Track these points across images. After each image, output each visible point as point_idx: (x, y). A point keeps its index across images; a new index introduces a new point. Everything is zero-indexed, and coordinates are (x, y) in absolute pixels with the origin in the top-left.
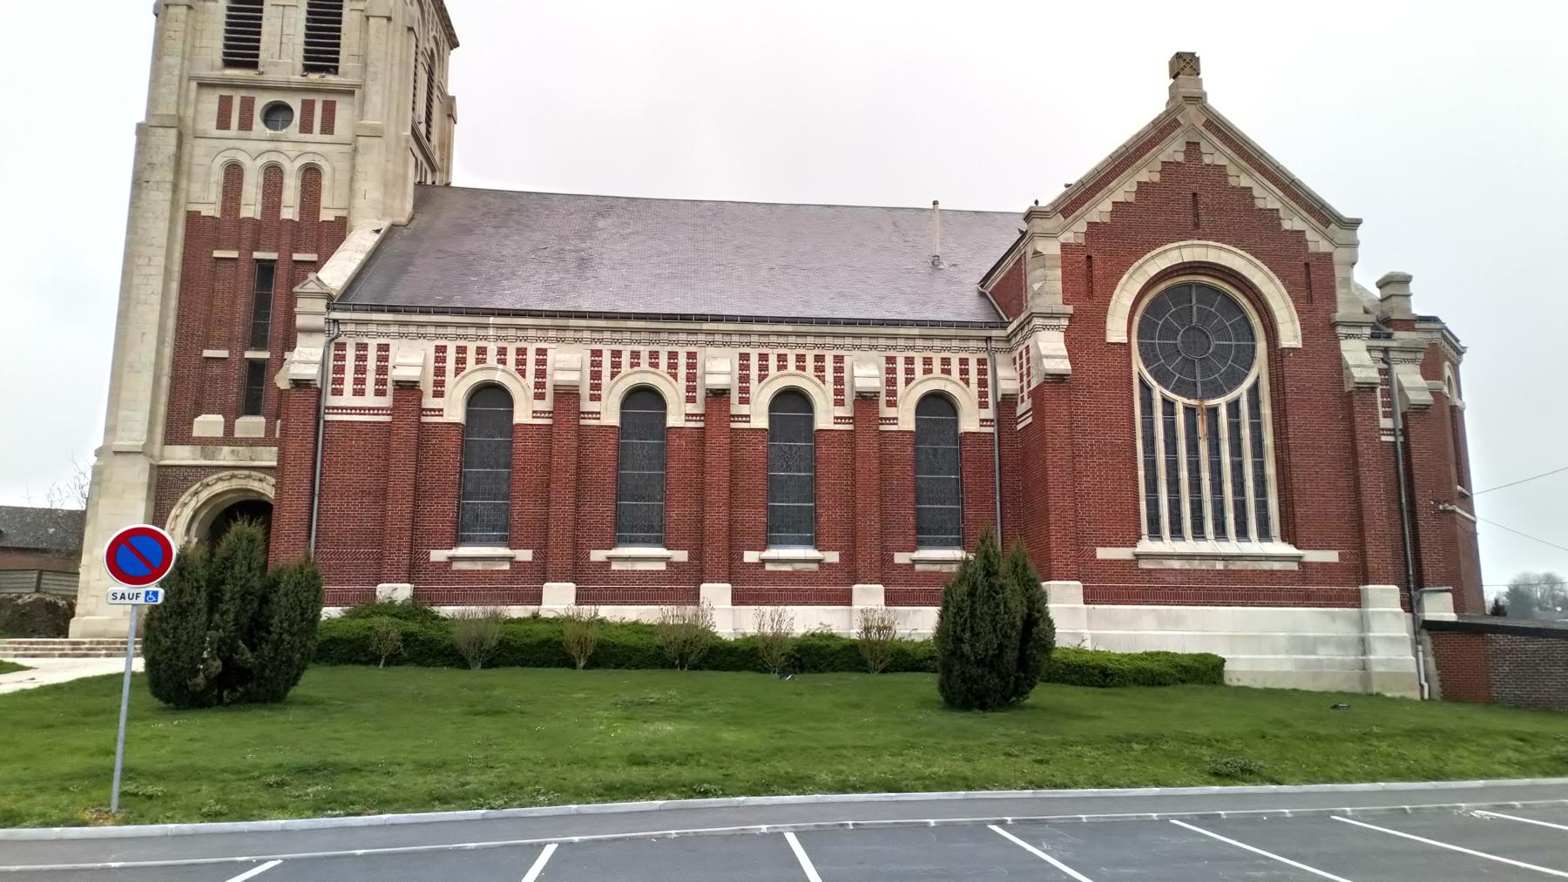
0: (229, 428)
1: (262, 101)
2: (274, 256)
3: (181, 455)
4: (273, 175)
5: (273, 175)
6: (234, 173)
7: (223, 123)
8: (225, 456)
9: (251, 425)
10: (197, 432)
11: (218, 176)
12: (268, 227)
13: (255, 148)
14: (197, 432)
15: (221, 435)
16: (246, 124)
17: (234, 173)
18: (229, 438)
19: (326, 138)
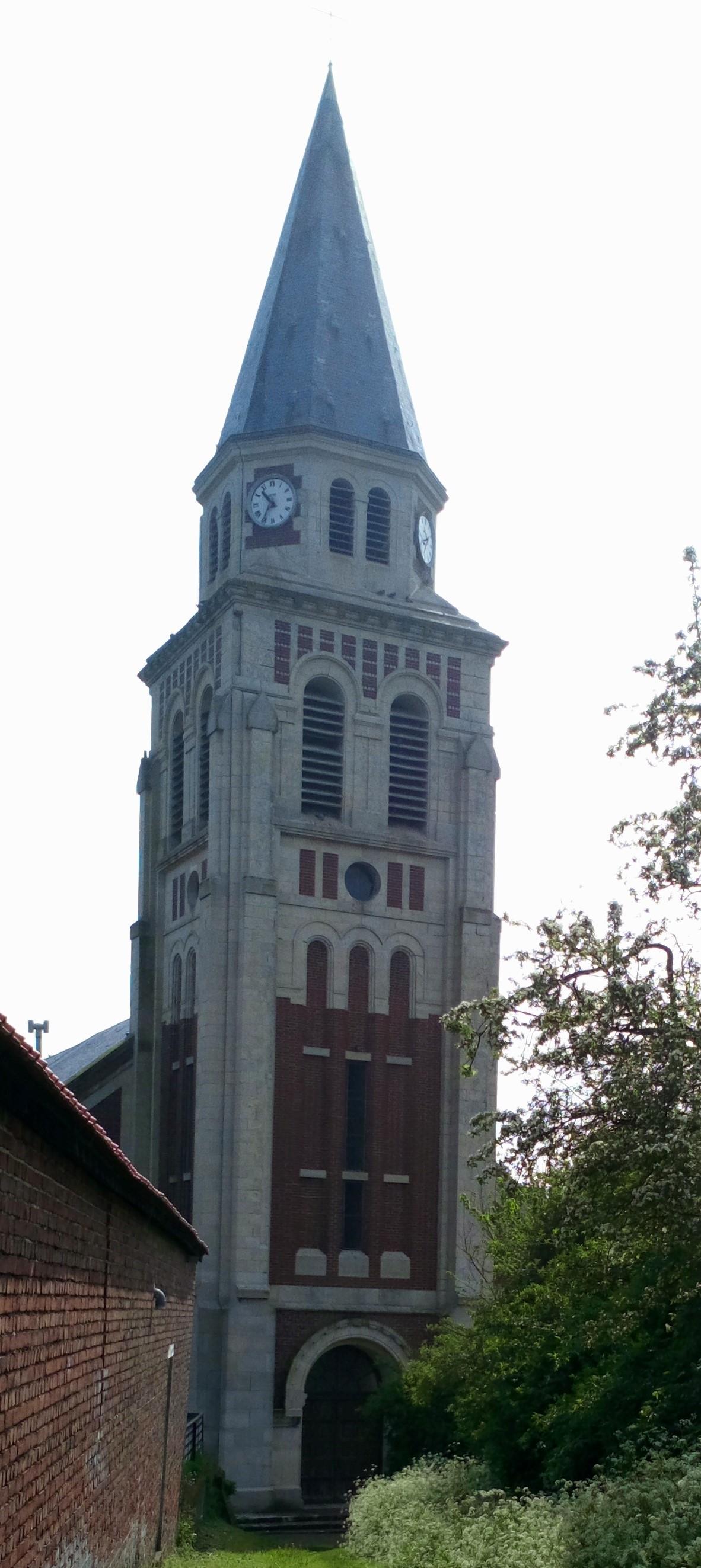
0: (332, 1264)
1: (346, 858)
2: (366, 1057)
3: (292, 1297)
4: (360, 956)
5: (360, 956)
6: (318, 951)
7: (307, 888)
8: (330, 1298)
9: (353, 1262)
10: (300, 1270)
11: (302, 952)
12: (356, 1021)
13: (336, 921)
14: (300, 1270)
15: (323, 1273)
16: (330, 891)
17: (318, 951)
18: (331, 1279)
19: (417, 914)
